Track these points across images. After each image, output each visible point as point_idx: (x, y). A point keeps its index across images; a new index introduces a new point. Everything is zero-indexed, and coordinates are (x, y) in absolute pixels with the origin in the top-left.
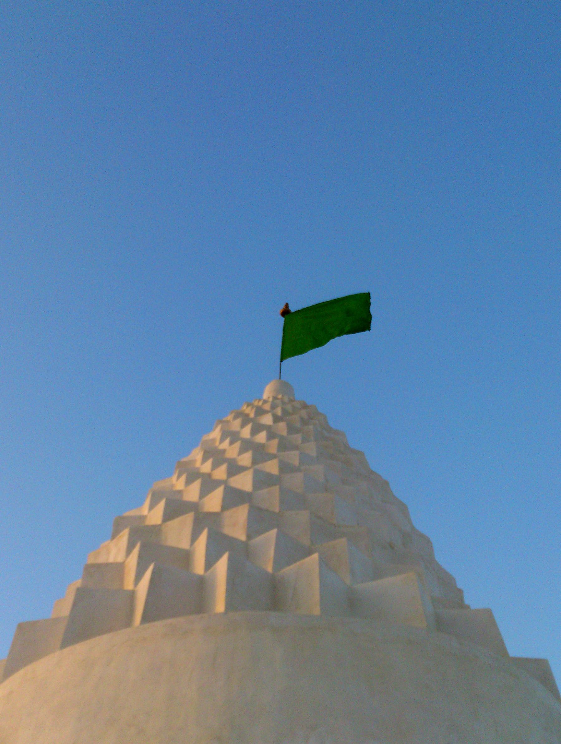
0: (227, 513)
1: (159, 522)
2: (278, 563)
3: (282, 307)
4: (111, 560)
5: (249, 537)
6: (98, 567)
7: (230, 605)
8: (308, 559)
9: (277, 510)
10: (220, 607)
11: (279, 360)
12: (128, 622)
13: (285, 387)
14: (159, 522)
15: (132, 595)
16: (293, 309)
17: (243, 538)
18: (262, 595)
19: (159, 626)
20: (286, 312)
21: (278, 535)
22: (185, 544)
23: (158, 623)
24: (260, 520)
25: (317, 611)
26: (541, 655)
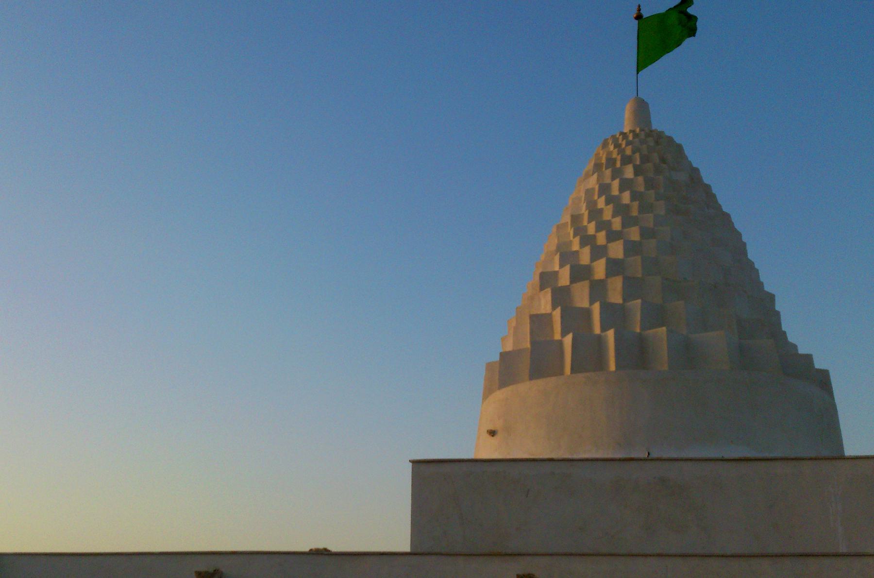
0: (609, 280)
1: (568, 283)
2: (643, 328)
3: (634, 13)
4: (543, 312)
5: (624, 300)
6: (537, 316)
7: (617, 367)
8: (660, 329)
9: (640, 276)
10: (612, 367)
11: (635, 69)
12: (561, 372)
13: (642, 109)
14: (568, 283)
15: (560, 343)
16: (646, 14)
17: (620, 301)
18: (635, 354)
19: (580, 377)
20: (639, 17)
21: (642, 304)
22: (585, 304)
23: (580, 375)
24: (632, 288)
25: (666, 368)
26: (773, 292)
